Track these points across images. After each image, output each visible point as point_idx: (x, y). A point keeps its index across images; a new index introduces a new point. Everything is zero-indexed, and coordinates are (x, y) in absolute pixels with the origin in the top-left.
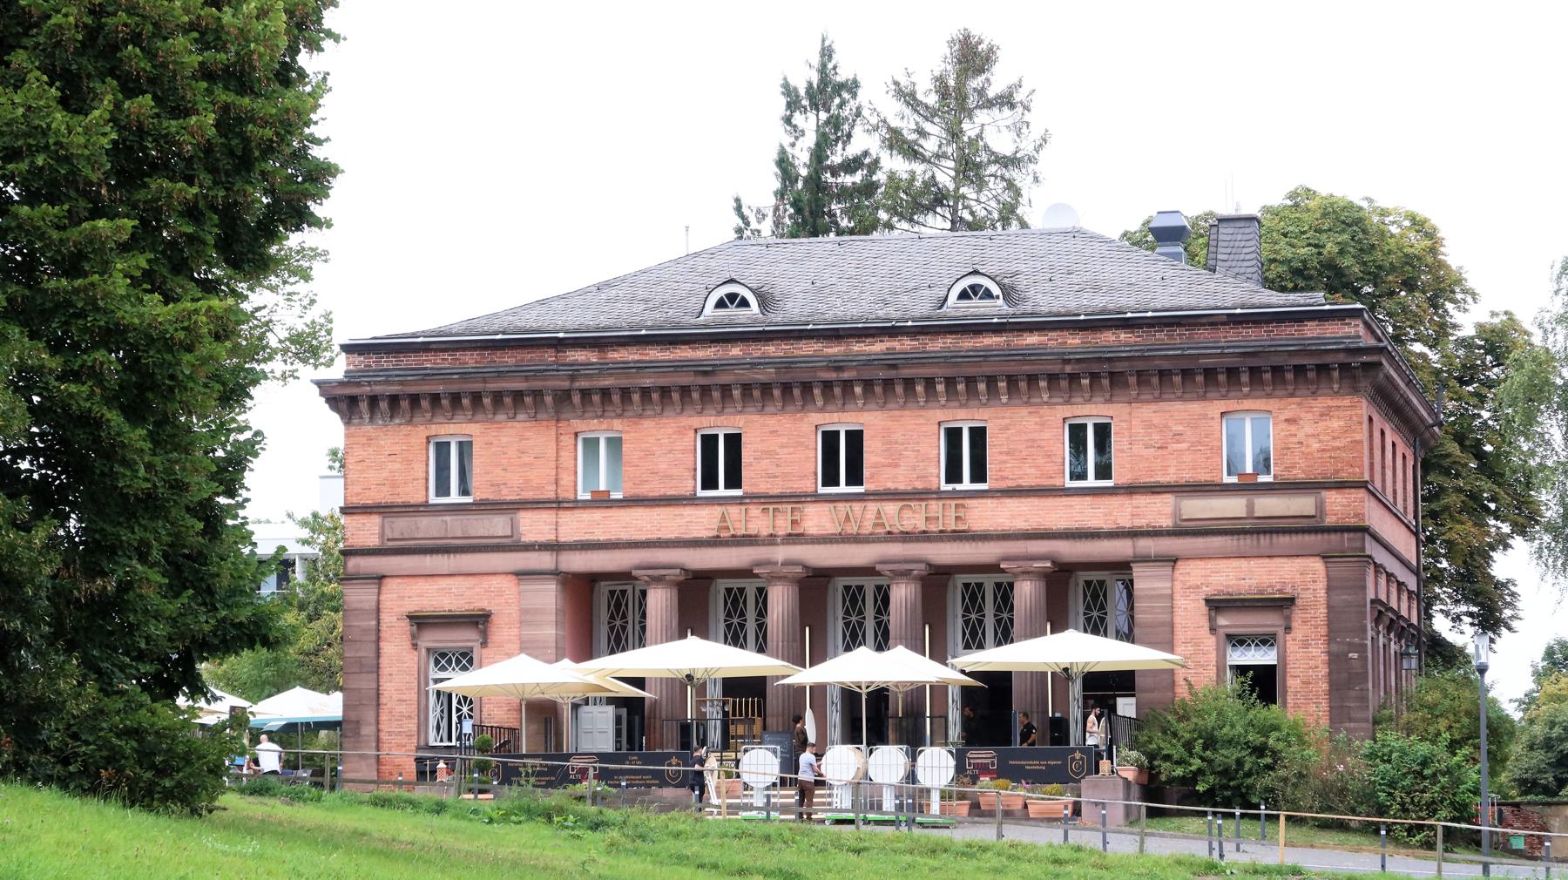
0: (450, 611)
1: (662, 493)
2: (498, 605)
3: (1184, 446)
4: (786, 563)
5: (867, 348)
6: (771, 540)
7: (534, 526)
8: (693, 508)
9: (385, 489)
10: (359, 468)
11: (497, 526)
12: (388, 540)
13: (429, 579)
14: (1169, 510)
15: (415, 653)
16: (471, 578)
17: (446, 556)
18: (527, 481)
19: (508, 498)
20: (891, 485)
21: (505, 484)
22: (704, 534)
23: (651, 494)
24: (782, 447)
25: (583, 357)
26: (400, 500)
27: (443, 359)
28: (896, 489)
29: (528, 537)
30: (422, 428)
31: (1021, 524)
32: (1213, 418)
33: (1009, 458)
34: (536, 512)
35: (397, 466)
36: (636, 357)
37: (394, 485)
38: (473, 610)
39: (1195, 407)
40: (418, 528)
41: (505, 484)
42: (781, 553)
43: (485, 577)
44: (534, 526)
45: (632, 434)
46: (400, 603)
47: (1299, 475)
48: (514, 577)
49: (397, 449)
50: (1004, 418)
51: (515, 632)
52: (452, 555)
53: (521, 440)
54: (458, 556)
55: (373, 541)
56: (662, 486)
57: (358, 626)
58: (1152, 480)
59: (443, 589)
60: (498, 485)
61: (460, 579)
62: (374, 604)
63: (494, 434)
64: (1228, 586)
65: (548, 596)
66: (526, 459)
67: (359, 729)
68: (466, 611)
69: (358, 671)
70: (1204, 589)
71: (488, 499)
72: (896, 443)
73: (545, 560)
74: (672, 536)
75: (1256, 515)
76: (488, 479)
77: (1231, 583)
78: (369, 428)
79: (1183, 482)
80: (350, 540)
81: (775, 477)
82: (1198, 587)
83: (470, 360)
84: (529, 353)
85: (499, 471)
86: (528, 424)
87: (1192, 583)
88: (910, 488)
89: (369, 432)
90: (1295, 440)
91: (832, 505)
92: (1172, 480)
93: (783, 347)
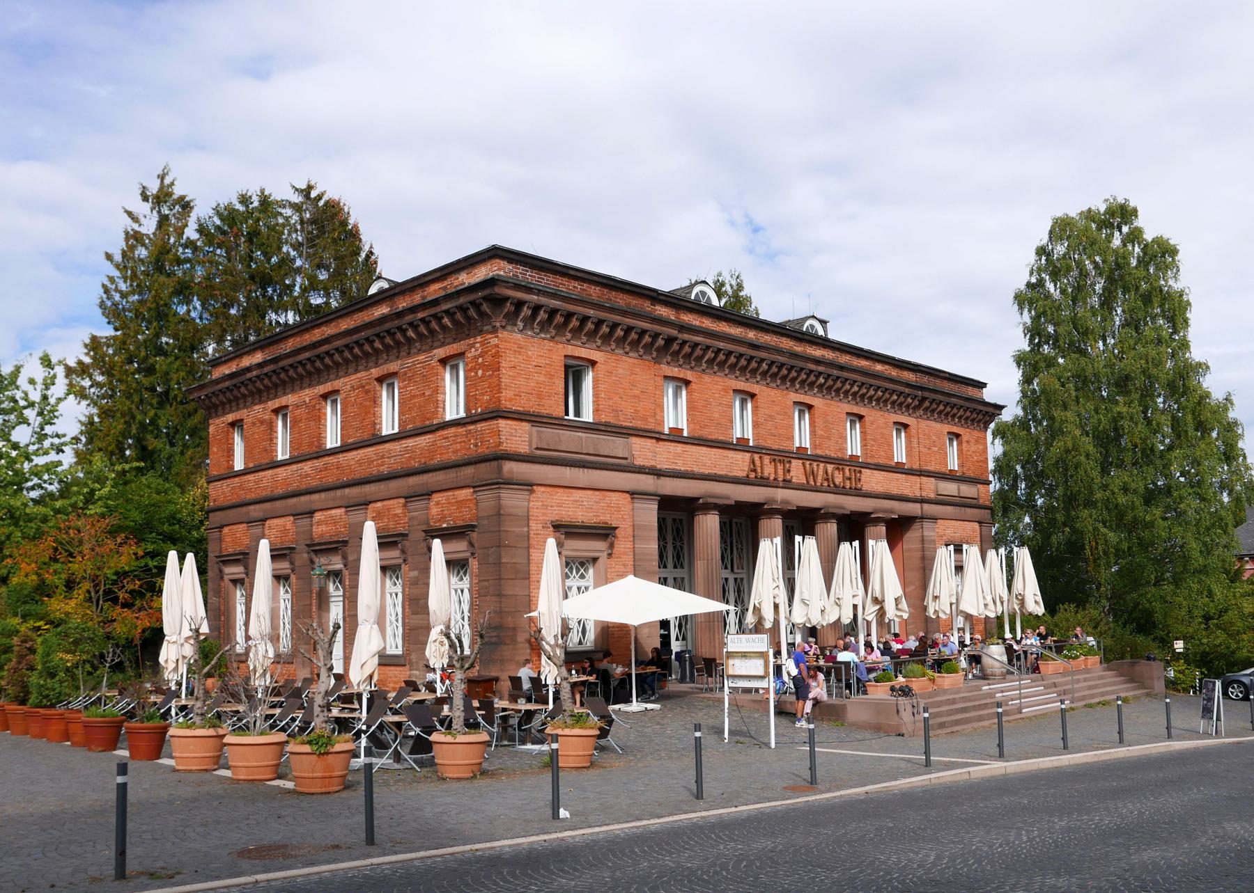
0: (582, 522)
3: (936, 449)
4: (784, 502)
6: (774, 484)
7: (643, 451)
8: (733, 452)
10: (511, 374)
11: (615, 446)
12: (537, 449)
13: (566, 490)
14: (933, 488)
16: (597, 493)
17: (581, 470)
19: (625, 424)
22: (741, 474)
23: (710, 437)
26: (545, 412)
27: (574, 287)
29: (639, 462)
30: (561, 346)
31: (879, 488)
34: (643, 440)
35: (542, 378)
36: (697, 323)
37: (540, 396)
38: (599, 523)
39: (938, 426)
40: (560, 441)
42: (781, 495)
43: (608, 493)
44: (643, 451)
49: (542, 361)
51: (630, 545)
52: (586, 470)
53: (632, 374)
55: (524, 449)
57: (514, 532)
59: (578, 501)
60: (617, 411)
61: (589, 492)
62: (526, 510)
65: (649, 513)
66: (637, 392)
68: (595, 523)
69: (513, 577)
71: (610, 422)
73: (646, 483)
74: (722, 473)
75: (962, 495)
83: (594, 292)
85: (617, 398)
86: (636, 361)
89: (519, 340)
90: (969, 453)
91: (801, 461)
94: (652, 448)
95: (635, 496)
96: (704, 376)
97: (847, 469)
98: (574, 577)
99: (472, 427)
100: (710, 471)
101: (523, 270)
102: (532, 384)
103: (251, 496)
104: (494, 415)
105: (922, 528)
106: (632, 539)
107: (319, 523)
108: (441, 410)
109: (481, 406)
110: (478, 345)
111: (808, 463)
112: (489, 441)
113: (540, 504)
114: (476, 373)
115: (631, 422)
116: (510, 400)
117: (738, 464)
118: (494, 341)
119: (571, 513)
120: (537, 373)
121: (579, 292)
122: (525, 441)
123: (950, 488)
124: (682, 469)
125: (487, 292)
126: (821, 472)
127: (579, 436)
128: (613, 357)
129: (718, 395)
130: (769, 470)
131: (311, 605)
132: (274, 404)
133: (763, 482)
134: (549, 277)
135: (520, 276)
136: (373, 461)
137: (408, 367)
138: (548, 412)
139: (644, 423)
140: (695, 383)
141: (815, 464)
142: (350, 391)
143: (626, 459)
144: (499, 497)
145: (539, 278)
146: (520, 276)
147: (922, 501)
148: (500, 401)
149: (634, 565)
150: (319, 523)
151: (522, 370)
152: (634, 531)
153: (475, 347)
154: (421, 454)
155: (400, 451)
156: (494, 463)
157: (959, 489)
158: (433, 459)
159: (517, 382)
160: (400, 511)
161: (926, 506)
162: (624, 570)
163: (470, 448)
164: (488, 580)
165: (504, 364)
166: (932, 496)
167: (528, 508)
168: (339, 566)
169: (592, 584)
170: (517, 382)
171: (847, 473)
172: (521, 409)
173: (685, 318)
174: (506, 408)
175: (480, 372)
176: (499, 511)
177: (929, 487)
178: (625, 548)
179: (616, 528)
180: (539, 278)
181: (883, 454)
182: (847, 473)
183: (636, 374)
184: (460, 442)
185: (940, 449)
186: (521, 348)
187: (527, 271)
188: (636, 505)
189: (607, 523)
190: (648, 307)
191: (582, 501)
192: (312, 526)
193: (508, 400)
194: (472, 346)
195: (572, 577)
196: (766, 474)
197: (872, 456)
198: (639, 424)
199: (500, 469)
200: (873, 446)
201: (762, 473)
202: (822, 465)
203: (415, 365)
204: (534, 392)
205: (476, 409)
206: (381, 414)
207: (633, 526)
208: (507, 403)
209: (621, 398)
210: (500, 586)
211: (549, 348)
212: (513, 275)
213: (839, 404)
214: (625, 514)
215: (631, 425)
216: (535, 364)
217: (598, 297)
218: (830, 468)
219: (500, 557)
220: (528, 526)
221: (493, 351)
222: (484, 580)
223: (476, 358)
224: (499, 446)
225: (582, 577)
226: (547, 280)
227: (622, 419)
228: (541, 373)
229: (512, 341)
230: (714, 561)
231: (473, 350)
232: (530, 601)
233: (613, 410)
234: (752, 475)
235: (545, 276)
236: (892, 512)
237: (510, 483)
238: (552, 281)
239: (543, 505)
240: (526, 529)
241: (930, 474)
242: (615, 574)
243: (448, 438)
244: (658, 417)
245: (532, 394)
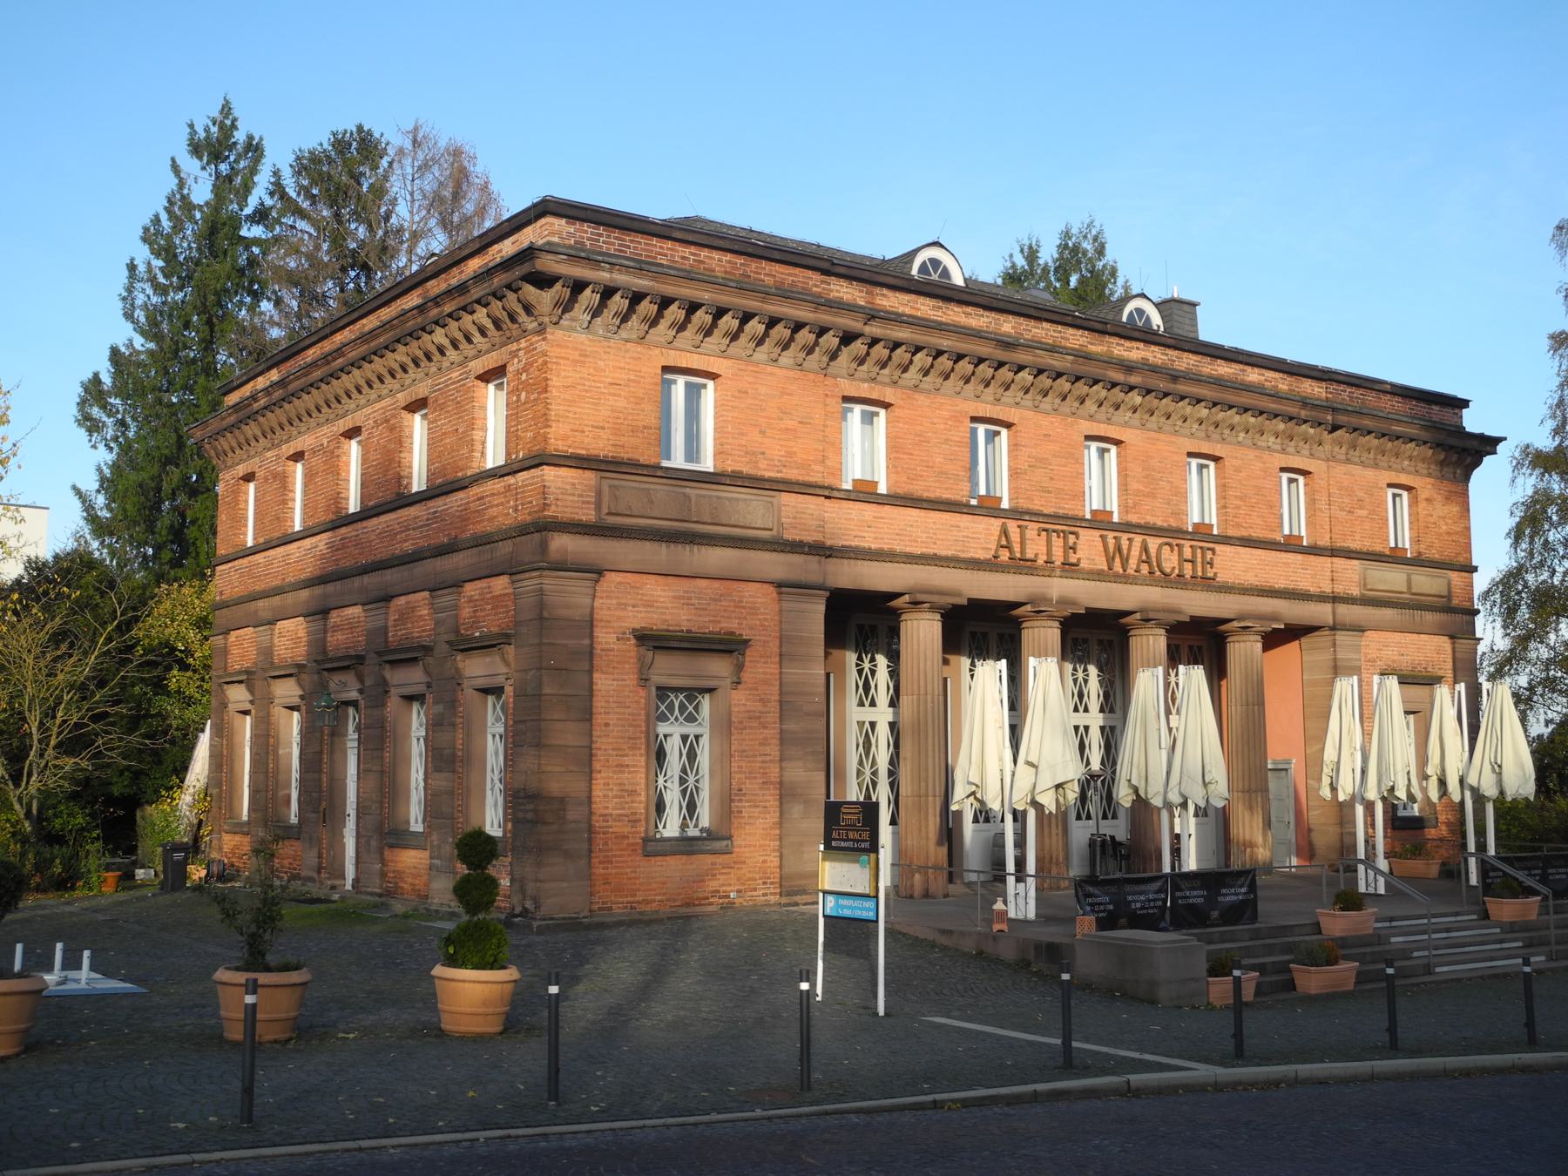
1: (938, 494)
2: (751, 628)
3: (1364, 513)
5: (1125, 354)
6: (1048, 568)
9: (605, 435)
10: (567, 397)
12: (610, 514)
14: (1356, 578)
15: (643, 693)
17: (688, 547)
18: (790, 454)
19: (767, 474)
20: (1151, 520)
21: (763, 453)
24: (1054, 456)
25: (849, 296)
28: (1155, 524)
30: (657, 351)
31: (1251, 579)
32: (1381, 488)
33: (1239, 503)
38: (719, 633)
39: (1370, 473)
40: (652, 502)
41: (763, 453)
45: (907, 411)
46: (621, 613)
47: (1434, 554)
48: (771, 589)
50: (1237, 458)
51: (773, 669)
52: (696, 547)
53: (783, 394)
54: (703, 549)
56: (937, 485)
58: (1345, 545)
60: (754, 453)
62: (588, 610)
63: (750, 379)
64: (1394, 661)
66: (791, 424)
67: (564, 810)
68: (710, 632)
70: (1379, 663)
71: (741, 472)
72: (1154, 470)
74: (950, 553)
75: (1414, 591)
76: (744, 443)
77: (1396, 658)
78: (583, 337)
79: (1365, 550)
80: (553, 508)
81: (1049, 492)
82: (1374, 661)
84: (789, 275)
86: (791, 374)
87: (1369, 656)
88: (1165, 525)
89: (582, 343)
90: (1432, 520)
91: (1097, 533)
92: (1358, 548)
93: (1052, 333)
94: (816, 513)
95: (784, 589)
96: (917, 396)
97: (1187, 544)
98: (676, 719)
100: (925, 550)
101: (592, 233)
102: (603, 413)
103: (259, 587)
104: (537, 462)
105: (1334, 645)
106: (777, 659)
107: (336, 628)
108: (478, 454)
109: (523, 449)
110: (521, 353)
111: (1111, 535)
112: (531, 502)
113: (614, 602)
115: (779, 472)
116: (565, 438)
117: (979, 536)
118: (541, 346)
119: (668, 617)
120: (614, 395)
121: (691, 266)
122: (588, 503)
123: (1391, 579)
124: (873, 546)
125: (524, 269)
126: (1135, 552)
127: (685, 494)
128: (750, 368)
129: (943, 426)
130: (1036, 547)
131: (321, 752)
132: (288, 449)
133: (1023, 565)
134: (639, 243)
135: (588, 243)
136: (396, 534)
137: (439, 389)
138: (630, 456)
139: (803, 472)
140: (900, 407)
141: (1124, 537)
142: (373, 428)
143: (771, 530)
145: (620, 245)
146: (588, 243)
147: (1335, 599)
148: (546, 439)
149: (781, 702)
150: (336, 628)
151: (587, 391)
152: (781, 646)
153: (517, 356)
154: (451, 524)
155: (428, 520)
157: (1409, 582)
159: (578, 410)
160: (426, 612)
161: (1342, 609)
162: (760, 709)
163: (508, 514)
164: (525, 721)
165: (555, 382)
166: (1355, 592)
167: (592, 608)
168: (354, 695)
169: (708, 730)
170: (578, 410)
171: (1187, 553)
172: (584, 452)
173: (885, 303)
174: (556, 450)
175: (523, 395)
176: (541, 613)
177: (1349, 576)
178: (764, 673)
179: (746, 642)
180: (620, 245)
181: (1259, 521)
182: (1187, 553)
183: (791, 395)
184: (497, 505)
185: (1372, 512)
186: (586, 356)
187: (601, 235)
188: (784, 604)
189: (732, 633)
190: (816, 286)
191: (690, 599)
192: (325, 632)
193: (559, 439)
194: (514, 354)
195: (672, 719)
196: (1030, 555)
197: (1238, 525)
198: (792, 474)
199: (544, 547)
200: (1238, 507)
201: (1023, 551)
202: (1138, 539)
203: (448, 386)
204: (606, 425)
205: (517, 452)
206: (411, 463)
207: (781, 638)
208: (560, 442)
209: (762, 432)
210: (540, 730)
211: (636, 355)
212: (576, 242)
213: (1174, 439)
214: (766, 620)
215: (779, 475)
216: (609, 380)
217: (726, 272)
218: (1153, 543)
220: (591, 636)
221: (540, 361)
222: (520, 721)
223: (519, 373)
224: (544, 510)
225: (691, 719)
226: (635, 248)
227: (761, 466)
228: (620, 395)
229: (570, 345)
230: (929, 697)
231: (516, 360)
232: (591, 755)
233: (747, 453)
234: (1004, 556)
235: (632, 241)
236: (1275, 619)
237: (561, 566)
238: (642, 249)
239: (618, 604)
240: (587, 642)
241: (1349, 554)
242: (746, 715)
243: (482, 498)
244: (829, 463)
245: (603, 428)
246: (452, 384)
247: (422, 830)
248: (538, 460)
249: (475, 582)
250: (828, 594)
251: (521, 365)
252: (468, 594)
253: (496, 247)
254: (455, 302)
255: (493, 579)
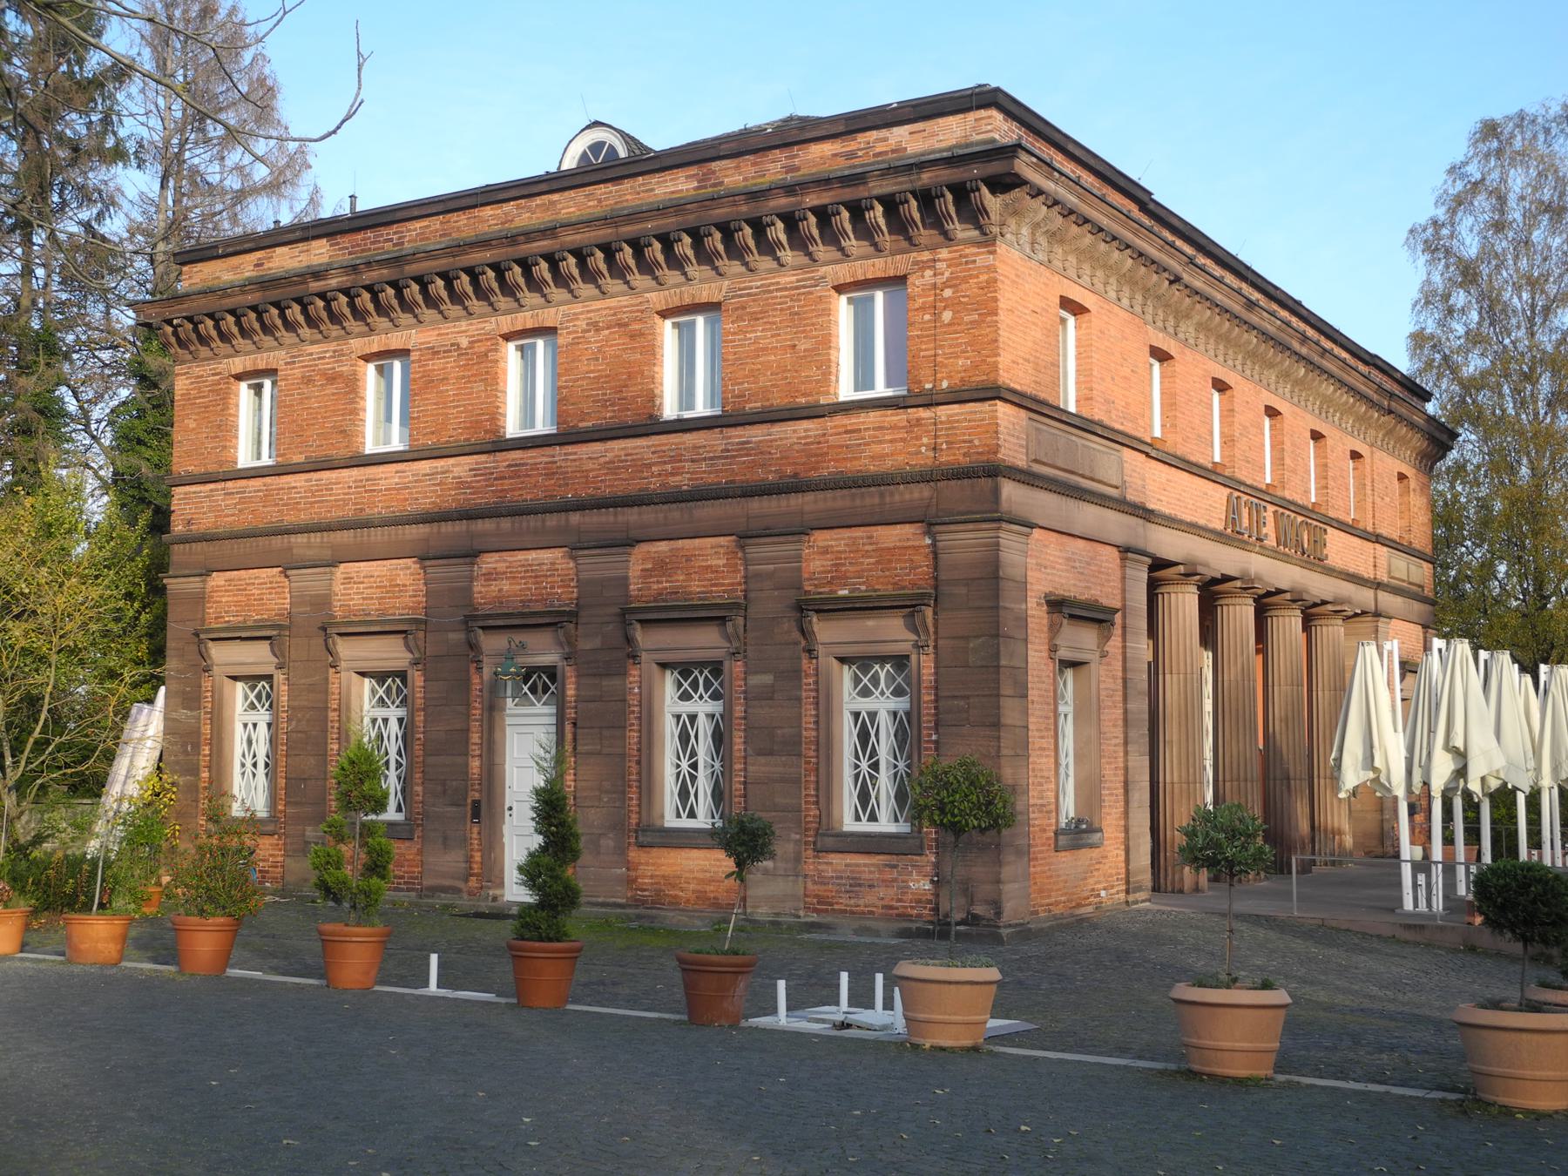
12: (1036, 461)
48: (1115, 550)
95: (1130, 555)
99: (924, 413)
104: (989, 395)
108: (833, 378)
109: (949, 377)
112: (971, 441)
114: (937, 316)
137: (749, 295)
144: (998, 544)
156: (986, 483)
158: (815, 469)
164: (968, 697)
194: (922, 266)
219: (997, 656)
221: (984, 278)
246: (777, 290)
247: (908, 830)
248: (992, 393)
249: (836, 531)
250: (1149, 561)
251: (940, 280)
252: (821, 544)
253: (873, 135)
254: (830, 194)
255: (879, 528)
